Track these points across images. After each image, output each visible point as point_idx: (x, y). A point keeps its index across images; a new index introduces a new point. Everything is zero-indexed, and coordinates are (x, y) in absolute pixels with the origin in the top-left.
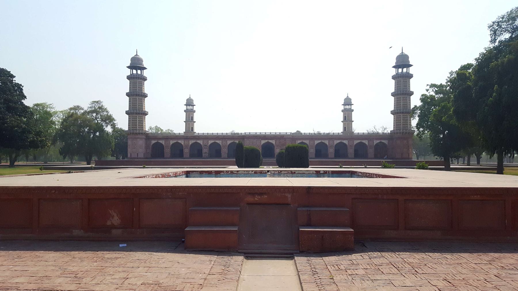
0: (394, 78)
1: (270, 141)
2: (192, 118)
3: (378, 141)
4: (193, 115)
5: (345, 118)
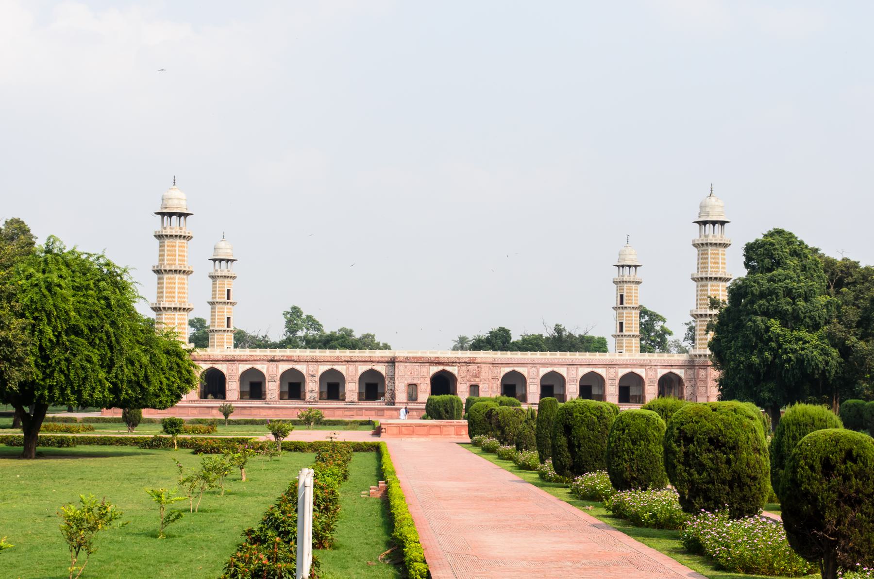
1: (448, 368)
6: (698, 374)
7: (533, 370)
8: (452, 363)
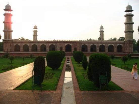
0: (125, 16)
1: (70, 44)
2: (36, 34)
4: (36, 33)
5: (101, 34)
7: (89, 44)
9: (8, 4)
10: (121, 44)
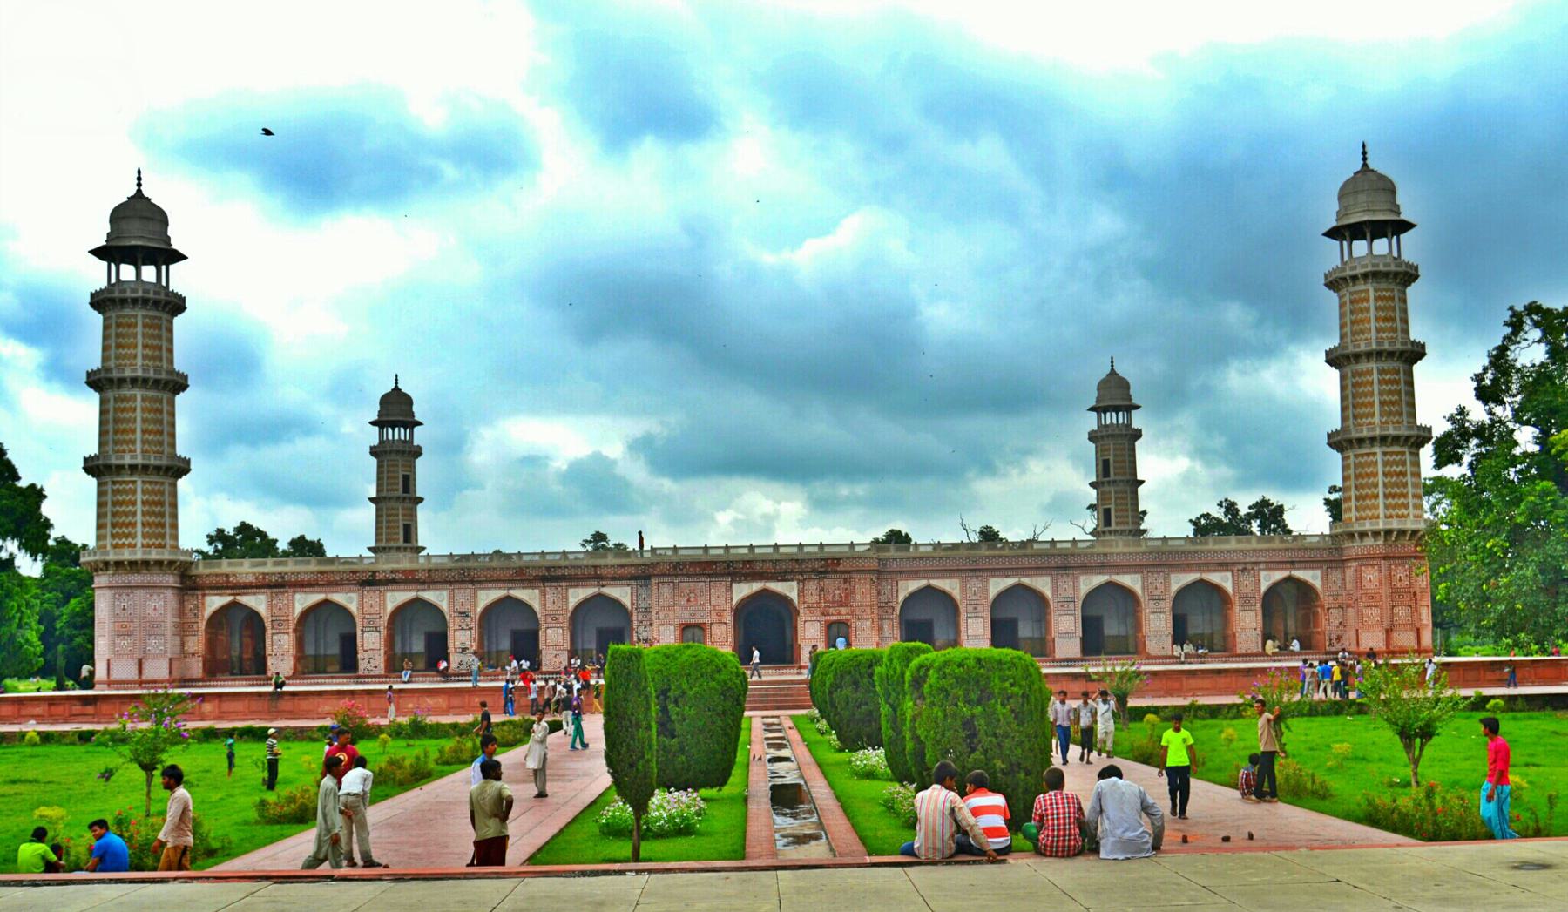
1: (775, 586)
2: (408, 482)
3: (1279, 575)
5: (1104, 468)
6: (1359, 581)
8: (783, 577)
9: (133, 192)
10: (1309, 564)
